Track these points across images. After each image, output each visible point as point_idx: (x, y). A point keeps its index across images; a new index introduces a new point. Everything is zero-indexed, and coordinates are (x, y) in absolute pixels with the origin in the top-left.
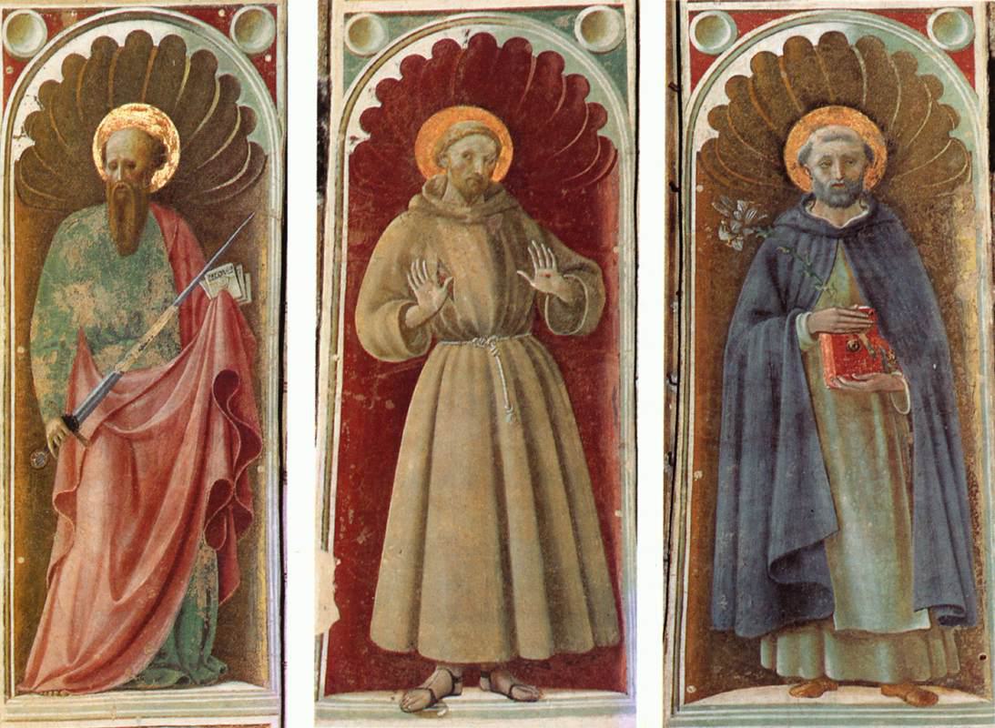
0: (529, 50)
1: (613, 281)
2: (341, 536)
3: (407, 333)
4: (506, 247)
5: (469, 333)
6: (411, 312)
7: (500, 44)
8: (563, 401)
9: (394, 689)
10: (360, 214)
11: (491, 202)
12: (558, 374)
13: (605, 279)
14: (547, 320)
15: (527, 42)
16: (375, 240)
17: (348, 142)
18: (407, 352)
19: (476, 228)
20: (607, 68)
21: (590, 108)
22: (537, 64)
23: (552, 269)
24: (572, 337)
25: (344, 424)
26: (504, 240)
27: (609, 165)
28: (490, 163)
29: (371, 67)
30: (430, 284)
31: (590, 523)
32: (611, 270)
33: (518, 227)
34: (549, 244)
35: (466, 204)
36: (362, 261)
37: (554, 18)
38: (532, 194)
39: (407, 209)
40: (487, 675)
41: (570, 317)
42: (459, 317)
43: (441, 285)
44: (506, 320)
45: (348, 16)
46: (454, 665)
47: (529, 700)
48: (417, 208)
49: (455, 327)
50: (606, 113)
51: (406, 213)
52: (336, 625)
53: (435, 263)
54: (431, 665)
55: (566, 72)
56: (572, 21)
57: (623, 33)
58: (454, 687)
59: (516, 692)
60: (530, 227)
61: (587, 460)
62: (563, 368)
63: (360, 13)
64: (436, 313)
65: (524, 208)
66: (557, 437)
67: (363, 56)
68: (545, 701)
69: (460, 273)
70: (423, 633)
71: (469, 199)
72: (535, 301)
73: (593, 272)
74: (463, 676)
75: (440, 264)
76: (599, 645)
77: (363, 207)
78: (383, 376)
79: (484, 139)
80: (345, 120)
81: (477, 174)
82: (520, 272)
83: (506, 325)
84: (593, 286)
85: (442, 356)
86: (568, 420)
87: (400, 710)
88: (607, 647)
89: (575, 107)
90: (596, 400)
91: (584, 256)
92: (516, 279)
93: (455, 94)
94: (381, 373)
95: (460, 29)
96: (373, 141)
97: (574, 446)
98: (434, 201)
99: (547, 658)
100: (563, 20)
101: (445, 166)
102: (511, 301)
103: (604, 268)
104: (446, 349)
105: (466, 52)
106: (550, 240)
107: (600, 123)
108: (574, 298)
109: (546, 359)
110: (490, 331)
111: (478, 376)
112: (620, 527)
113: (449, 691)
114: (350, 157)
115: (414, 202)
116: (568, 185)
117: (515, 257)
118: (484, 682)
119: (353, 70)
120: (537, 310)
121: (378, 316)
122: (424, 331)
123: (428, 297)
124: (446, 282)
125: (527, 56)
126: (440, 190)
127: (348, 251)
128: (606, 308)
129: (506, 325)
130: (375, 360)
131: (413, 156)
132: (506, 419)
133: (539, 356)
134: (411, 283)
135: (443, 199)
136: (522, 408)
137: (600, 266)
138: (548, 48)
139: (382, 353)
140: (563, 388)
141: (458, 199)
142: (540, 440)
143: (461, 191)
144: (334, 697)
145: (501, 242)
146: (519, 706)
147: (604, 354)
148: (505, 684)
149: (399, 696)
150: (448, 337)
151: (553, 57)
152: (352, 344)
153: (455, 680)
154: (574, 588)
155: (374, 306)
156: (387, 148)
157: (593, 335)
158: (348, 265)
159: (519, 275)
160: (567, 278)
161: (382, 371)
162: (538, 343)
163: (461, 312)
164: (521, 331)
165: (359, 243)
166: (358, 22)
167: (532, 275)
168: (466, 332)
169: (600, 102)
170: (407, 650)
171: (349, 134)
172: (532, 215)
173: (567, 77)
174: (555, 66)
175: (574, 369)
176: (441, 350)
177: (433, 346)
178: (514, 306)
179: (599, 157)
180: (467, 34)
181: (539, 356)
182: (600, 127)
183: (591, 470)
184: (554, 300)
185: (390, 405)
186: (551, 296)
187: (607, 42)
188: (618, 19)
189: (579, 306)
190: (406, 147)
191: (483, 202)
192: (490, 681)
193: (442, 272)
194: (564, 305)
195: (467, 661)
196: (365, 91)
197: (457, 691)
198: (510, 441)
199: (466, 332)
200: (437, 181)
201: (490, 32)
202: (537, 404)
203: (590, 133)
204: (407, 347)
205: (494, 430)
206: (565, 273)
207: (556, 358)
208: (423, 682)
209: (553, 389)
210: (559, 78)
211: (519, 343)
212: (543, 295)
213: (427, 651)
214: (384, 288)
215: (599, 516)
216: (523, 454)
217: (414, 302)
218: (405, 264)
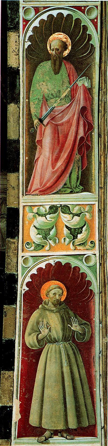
2: (21, 395)
3: (38, 341)
4: (65, 318)
5: (55, 341)
7: (63, 265)
9: (36, 436)
11: (61, 307)
13: (91, 327)
16: (30, 316)
17: (23, 290)
19: (57, 313)
26: (64, 316)
28: (61, 296)
30: (45, 328)
31: (87, 392)
33: (68, 314)
34: (76, 318)
35: (54, 307)
39: (38, 308)
40: (60, 432)
42: (52, 337)
43: (48, 329)
44: (65, 338)
45: (23, 257)
46: (51, 430)
54: (46, 430)
55: (80, 272)
58: (51, 436)
60: (71, 313)
62: (80, 350)
64: (46, 336)
65: (70, 308)
66: (78, 369)
71: (55, 305)
74: (54, 433)
75: (47, 323)
78: (32, 353)
79: (59, 289)
80: (22, 285)
81: (57, 299)
82: (68, 325)
83: (65, 339)
85: (48, 348)
86: (81, 364)
88: (92, 425)
91: (85, 321)
92: (67, 327)
96: (29, 290)
97: (83, 372)
98: (46, 306)
100: (80, 258)
101: (48, 297)
103: (91, 324)
104: (49, 345)
105: (54, 266)
109: (76, 348)
110: (61, 341)
115: (40, 306)
116: (82, 302)
117: (67, 321)
124: (49, 328)
125: (70, 267)
127: (23, 319)
129: (65, 339)
132: (65, 364)
136: (69, 361)
138: (76, 265)
139: (32, 347)
140: (80, 355)
141: (52, 306)
144: (20, 438)
146: (68, 441)
147: (91, 347)
148: (65, 435)
149: (37, 438)
150: (50, 342)
151: (77, 267)
152: (24, 344)
153: (52, 434)
154: (83, 409)
155: (30, 334)
158: (23, 323)
159: (69, 326)
160: (81, 327)
164: (69, 341)
165: (26, 317)
166: (25, 258)
167: (72, 327)
171: (23, 288)
174: (78, 270)
180: (54, 262)
185: (34, 361)
186: (77, 331)
187: (91, 264)
189: (84, 334)
193: (48, 325)
194: (80, 334)
195: (55, 429)
198: (66, 369)
202: (73, 360)
203: (87, 288)
205: (62, 367)
208: (43, 435)
209: (77, 356)
212: (75, 331)
214: (32, 329)
216: (70, 374)
217: (41, 333)
218: (38, 323)
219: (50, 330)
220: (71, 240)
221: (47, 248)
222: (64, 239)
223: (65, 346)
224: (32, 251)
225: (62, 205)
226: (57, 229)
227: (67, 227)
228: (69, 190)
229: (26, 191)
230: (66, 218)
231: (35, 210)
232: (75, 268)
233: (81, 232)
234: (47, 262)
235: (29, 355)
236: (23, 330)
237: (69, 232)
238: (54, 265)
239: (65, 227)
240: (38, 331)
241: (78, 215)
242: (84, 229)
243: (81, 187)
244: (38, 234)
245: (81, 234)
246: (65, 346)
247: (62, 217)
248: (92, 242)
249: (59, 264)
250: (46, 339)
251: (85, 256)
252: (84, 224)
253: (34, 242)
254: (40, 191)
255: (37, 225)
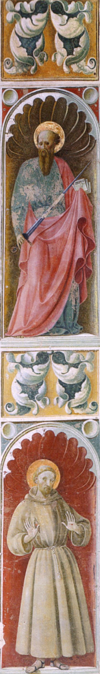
0: (66, 437)
1: (94, 527)
2: (5, 617)
3: (24, 545)
4: (58, 513)
5: (45, 545)
6: (26, 536)
7: (56, 435)
8: (77, 570)
9: (24, 666)
10: (8, 501)
11: (52, 497)
12: (75, 560)
13: (91, 525)
14: (72, 541)
15: (65, 434)
16: (13, 511)
17: (3, 473)
18: (24, 552)
19: (47, 506)
20: (93, 444)
21: (87, 461)
22: (69, 443)
23: (74, 522)
24: (80, 547)
25: (4, 578)
26: (57, 510)
27: (93, 483)
28: (53, 482)
29: (11, 444)
31: (85, 612)
32: (93, 522)
33: (62, 507)
34: (73, 513)
35: (44, 497)
36: (9, 519)
37: (75, 424)
38: (67, 494)
39: (24, 499)
40: (53, 662)
41: (79, 539)
42: (42, 539)
43: (36, 528)
44: (58, 540)
46: (42, 659)
47: (65, 669)
48: (27, 499)
49: (41, 543)
50: (92, 462)
51: (23, 501)
52: (4, 646)
53: (34, 519)
54: (35, 658)
55: (78, 446)
56: (81, 425)
57: (99, 430)
58: (42, 666)
59: (62, 667)
60: (66, 506)
61: (85, 591)
62: (77, 558)
63: (7, 422)
64: (34, 538)
65: (64, 499)
66: (75, 583)
67: (8, 439)
68: (70, 669)
69: (42, 524)
70: (32, 649)
71: (45, 495)
72: (68, 534)
73: (88, 523)
74: (45, 662)
75: (35, 520)
76: (88, 652)
77: (9, 499)
78: (17, 561)
79: (50, 472)
81: (48, 486)
82: (63, 523)
83: (58, 542)
84: (87, 528)
85: (36, 554)
86: (78, 577)
87: (25, 673)
89: (82, 460)
90: (88, 570)
91: (84, 517)
92: (61, 525)
93: (40, 455)
94: (16, 560)
95: (42, 428)
96: (12, 473)
97: (81, 587)
98: (33, 496)
99: (72, 656)
100: (78, 425)
101: (37, 483)
102: (59, 534)
103: (91, 522)
104: (38, 551)
105: (44, 438)
106: (73, 511)
107: (90, 466)
108: (81, 532)
109: (71, 554)
110: (52, 544)
111: (49, 561)
112: (95, 614)
113: (41, 666)
114: (4, 479)
115: (26, 496)
116: (79, 490)
117: (61, 518)
118: (51, 664)
119: (5, 445)
120: (68, 536)
121: (14, 539)
122: (30, 544)
123: (31, 531)
125: (65, 439)
126: (35, 492)
127: (4, 515)
128: (92, 536)
129: (58, 542)
130: (14, 555)
131: (26, 479)
132: (58, 577)
133: (69, 554)
134: (26, 527)
135: (37, 495)
136: (63, 573)
137: (90, 521)
138: (73, 436)
139: (16, 553)
140: (77, 565)
141: (42, 496)
142: (69, 584)
143: (42, 493)
144: (4, 668)
145: (56, 512)
147: (91, 553)
148: (58, 665)
149: (25, 668)
150: (38, 546)
151: (74, 440)
153: (42, 663)
154: (80, 634)
155: (13, 536)
156: (17, 476)
157: (87, 546)
158: (4, 520)
159: (62, 524)
160: (79, 525)
161: (16, 559)
162: (69, 549)
163: (43, 538)
164: (63, 544)
165: (8, 512)
166: (6, 425)
167: (67, 524)
168: (44, 545)
169: (90, 458)
170: (27, 654)
171: (4, 470)
172: (67, 502)
173: (79, 448)
174: (75, 443)
175: (81, 559)
176: (36, 551)
177: (33, 550)
178: (61, 535)
179: (90, 480)
180: (44, 431)
181: (69, 554)
182: (90, 468)
183: (86, 594)
184: (74, 533)
185: (19, 571)
186: (73, 532)
188: (97, 424)
189: (82, 535)
190: (23, 475)
191: (50, 496)
192: (53, 663)
193: (36, 523)
194: (78, 535)
195: (46, 657)
196: (9, 453)
197: (43, 666)
198: (60, 584)
199: (44, 545)
200: (34, 489)
201: (52, 430)
202: (68, 571)
203: (87, 470)
204: (25, 550)
205: (54, 580)
206: (78, 523)
207: (75, 554)
208: (33, 664)
209: (74, 566)
210: (76, 447)
211: (62, 549)
212: (71, 531)
213: (33, 654)
214: (17, 529)
215: (88, 610)
216: (64, 589)
218: (23, 520)
219: (39, 531)
220: (66, 400)
221: (34, 411)
222: (58, 399)
223: (58, 551)
224: (14, 415)
225: (55, 352)
226: (47, 386)
227: (61, 383)
228: (64, 331)
229: (6, 331)
230: (59, 369)
231: (18, 358)
232: (71, 439)
233: (79, 390)
234: (34, 432)
235: (12, 564)
236: (5, 529)
237: (63, 389)
238: (44, 436)
239: (58, 382)
240: (24, 530)
241: (76, 366)
242: (83, 385)
243: (80, 327)
244: (23, 392)
245: (80, 392)
246: (58, 551)
247: (54, 368)
248: (94, 404)
249: (50, 434)
250: (33, 542)
251: (85, 423)
252: (83, 379)
253: (17, 404)
254: (24, 332)
255: (21, 380)
